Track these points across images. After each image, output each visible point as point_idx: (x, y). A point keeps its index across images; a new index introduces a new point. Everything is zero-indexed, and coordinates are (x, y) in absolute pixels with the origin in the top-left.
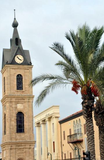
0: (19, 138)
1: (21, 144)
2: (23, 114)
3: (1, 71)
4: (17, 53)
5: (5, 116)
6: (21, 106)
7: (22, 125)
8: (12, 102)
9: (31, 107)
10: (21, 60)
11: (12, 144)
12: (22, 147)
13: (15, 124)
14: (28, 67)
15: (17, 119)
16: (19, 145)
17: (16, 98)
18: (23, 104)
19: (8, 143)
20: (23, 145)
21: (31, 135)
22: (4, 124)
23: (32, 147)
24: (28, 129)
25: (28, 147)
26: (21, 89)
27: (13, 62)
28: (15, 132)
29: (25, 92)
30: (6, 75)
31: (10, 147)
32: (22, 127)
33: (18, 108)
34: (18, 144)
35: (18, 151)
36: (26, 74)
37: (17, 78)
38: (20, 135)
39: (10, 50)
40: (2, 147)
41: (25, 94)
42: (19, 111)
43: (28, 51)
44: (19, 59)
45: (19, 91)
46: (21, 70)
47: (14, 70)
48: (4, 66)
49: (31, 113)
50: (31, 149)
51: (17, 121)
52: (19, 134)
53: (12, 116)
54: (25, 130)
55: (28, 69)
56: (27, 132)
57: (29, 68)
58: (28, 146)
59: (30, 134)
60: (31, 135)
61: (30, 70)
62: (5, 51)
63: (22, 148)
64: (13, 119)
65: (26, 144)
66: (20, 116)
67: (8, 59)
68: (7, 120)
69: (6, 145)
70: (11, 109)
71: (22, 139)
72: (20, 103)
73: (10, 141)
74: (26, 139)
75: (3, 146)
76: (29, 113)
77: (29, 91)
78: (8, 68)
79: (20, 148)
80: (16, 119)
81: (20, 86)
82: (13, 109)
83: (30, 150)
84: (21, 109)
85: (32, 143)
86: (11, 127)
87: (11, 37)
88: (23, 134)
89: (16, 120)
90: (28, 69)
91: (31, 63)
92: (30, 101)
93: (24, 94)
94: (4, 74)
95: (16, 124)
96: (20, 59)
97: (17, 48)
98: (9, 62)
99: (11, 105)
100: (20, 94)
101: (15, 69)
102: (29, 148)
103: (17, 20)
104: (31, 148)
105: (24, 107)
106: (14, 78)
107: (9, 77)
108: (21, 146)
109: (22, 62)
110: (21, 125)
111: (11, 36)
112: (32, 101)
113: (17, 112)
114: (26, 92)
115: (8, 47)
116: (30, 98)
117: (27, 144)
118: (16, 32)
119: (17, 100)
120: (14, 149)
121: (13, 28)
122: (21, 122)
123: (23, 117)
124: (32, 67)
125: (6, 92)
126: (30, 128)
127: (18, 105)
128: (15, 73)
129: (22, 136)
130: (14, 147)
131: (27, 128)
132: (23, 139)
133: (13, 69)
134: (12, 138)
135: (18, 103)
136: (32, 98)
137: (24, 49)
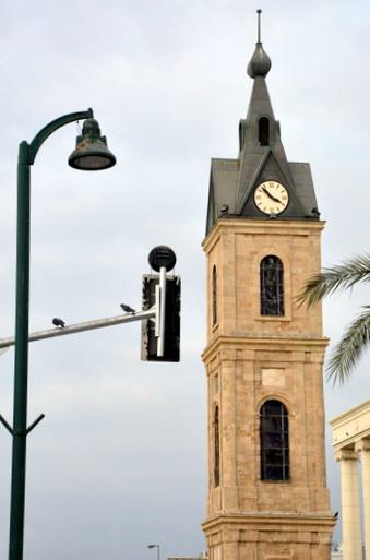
0: (271, 501)
2: (285, 407)
3: (203, 244)
4: (265, 175)
5: (217, 414)
6: (277, 380)
7: (280, 452)
8: (243, 360)
9: (315, 382)
10: (277, 200)
11: (243, 523)
12: (283, 538)
13: (253, 448)
15: (261, 429)
18: (283, 369)
19: (229, 520)
20: (284, 528)
21: (316, 491)
22: (212, 443)
24: (304, 466)
25: (305, 536)
27: (249, 211)
30: (221, 257)
31: (236, 536)
32: (281, 458)
33: (264, 383)
34: (267, 525)
35: (266, 553)
36: (299, 254)
37: (261, 270)
39: (239, 165)
40: (209, 533)
41: (292, 334)
42: (271, 398)
43: (308, 164)
44: (269, 196)
45: (268, 318)
46: (277, 238)
47: (250, 238)
48: (214, 223)
49: (315, 404)
51: (261, 435)
52: (271, 486)
53: (243, 415)
54: (294, 472)
55: (306, 236)
56: (301, 479)
57: (306, 233)
58: (305, 536)
59: (312, 489)
60: (316, 491)
61: (311, 238)
62: (218, 166)
63: (284, 540)
64: (246, 428)
65: (296, 524)
66: (274, 416)
67: (231, 198)
68: (226, 429)
69: (222, 527)
70: (239, 388)
73: (235, 510)
75: (211, 528)
76: (308, 404)
77: (308, 318)
78: (229, 230)
79: (275, 539)
80: (258, 427)
81: (272, 301)
83: (315, 552)
84: (276, 388)
85: (323, 525)
86: (241, 458)
87: (244, 116)
88: (285, 485)
89: (258, 433)
91: (315, 210)
92: (312, 359)
93: (287, 333)
94: (212, 254)
95: (259, 448)
96: (272, 198)
97: (263, 158)
98: (231, 211)
99: (239, 372)
100: (273, 331)
101: (254, 235)
102: (311, 544)
103: (267, 49)
105: (290, 382)
106: (250, 270)
107: (232, 267)
108: (280, 531)
109: (282, 208)
110: (276, 451)
111: (241, 110)
112: (319, 360)
113: (260, 399)
115: (231, 150)
116: (313, 349)
118: (260, 96)
119: (262, 356)
121: (252, 80)
122: (276, 441)
123: (286, 420)
124: (321, 229)
125: (221, 322)
126: (314, 465)
127: (264, 370)
128: (253, 249)
129: (283, 496)
130: (251, 534)
131: (300, 465)
132: (288, 506)
133: (246, 234)
134: (244, 499)
135: (267, 365)
136: (319, 349)
137: (289, 159)
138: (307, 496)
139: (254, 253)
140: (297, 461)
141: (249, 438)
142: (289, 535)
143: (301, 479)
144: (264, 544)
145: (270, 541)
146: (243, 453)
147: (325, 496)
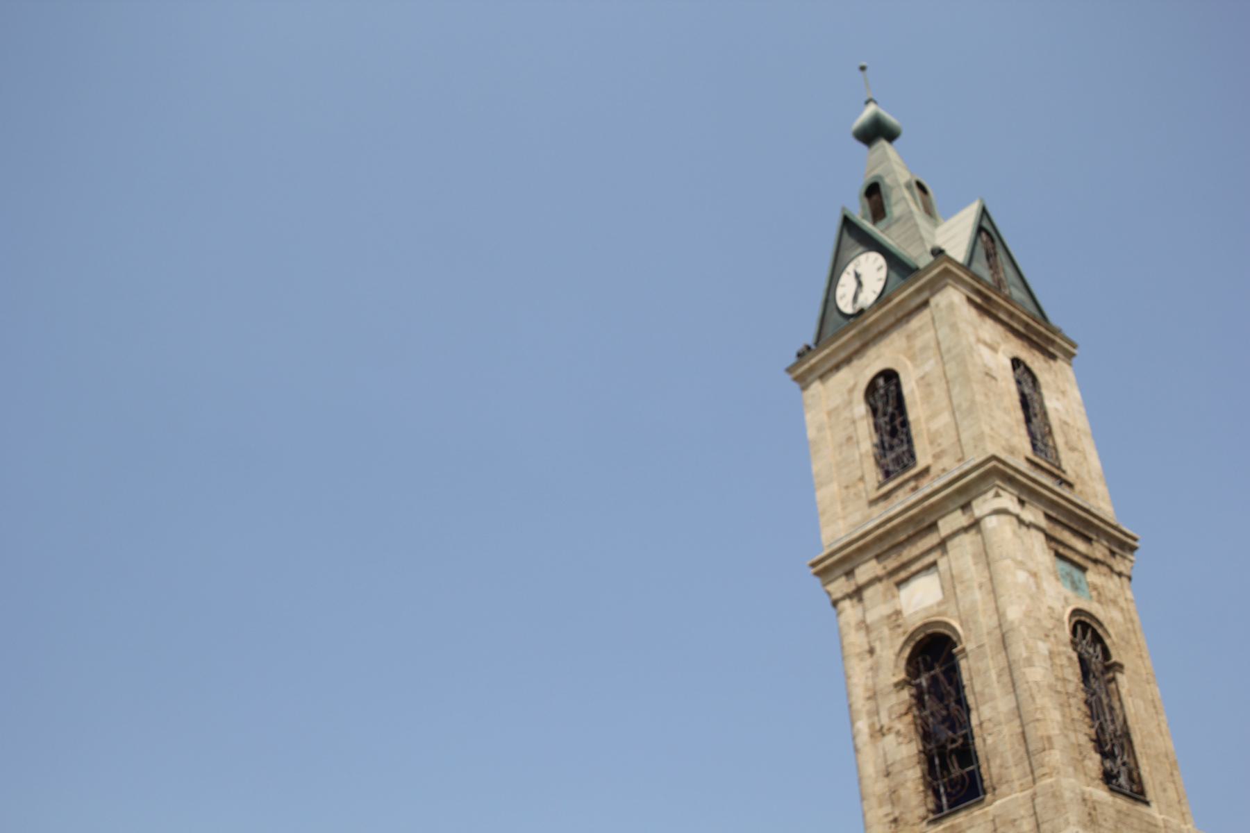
14: (919, 291)
17: (877, 551)
21: (1033, 797)
26: (906, 468)
29: (933, 471)
36: (918, 343)
54: (990, 769)
64: (885, 720)
72: (914, 568)
78: (809, 379)
82: (874, 635)
90: (925, 304)
105: (951, 586)
114: (947, 462)
119: (892, 563)
128: (851, 383)
135: (903, 575)
139: (851, 391)
141: (890, 739)
147: (1054, 795)
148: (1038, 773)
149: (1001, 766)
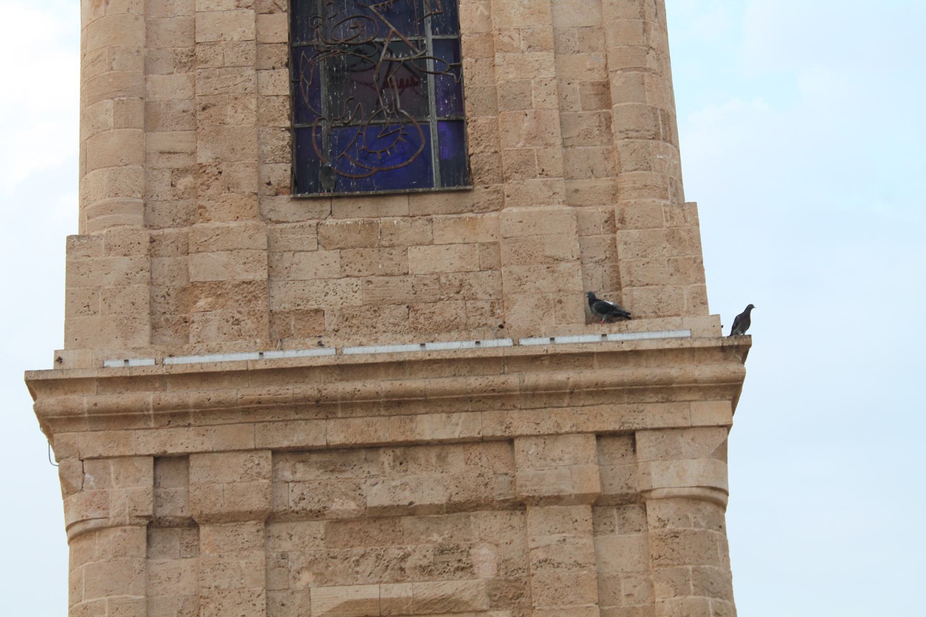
1: (399, 403)
12: (427, 485)
16: (335, 432)
20: (430, 426)
21: (612, 223)
23: (667, 473)
28: (249, 185)
31: (129, 491)
34: (322, 417)
35: (322, 580)
38: (373, 238)
50: (654, 511)
52: (349, 215)
56: (524, 166)
59: (597, 213)
60: (612, 223)
71: (417, 318)
74: (519, 312)
79: (378, 496)
83: (623, 549)
85: (666, 390)
88: (433, 203)
95: (279, 27)
104: (637, 500)
117: (552, 395)
120: (235, 518)
126: (604, 89)
129: (420, 261)
130: (228, 476)
132: (453, 310)
134: (190, 290)
138: (569, 246)
140: (506, 74)
142: (457, 460)
143: (524, 166)
144: (318, 527)
145: (343, 506)
146: (189, 61)
147: (672, 236)
148: (627, 180)
149: (532, 138)
